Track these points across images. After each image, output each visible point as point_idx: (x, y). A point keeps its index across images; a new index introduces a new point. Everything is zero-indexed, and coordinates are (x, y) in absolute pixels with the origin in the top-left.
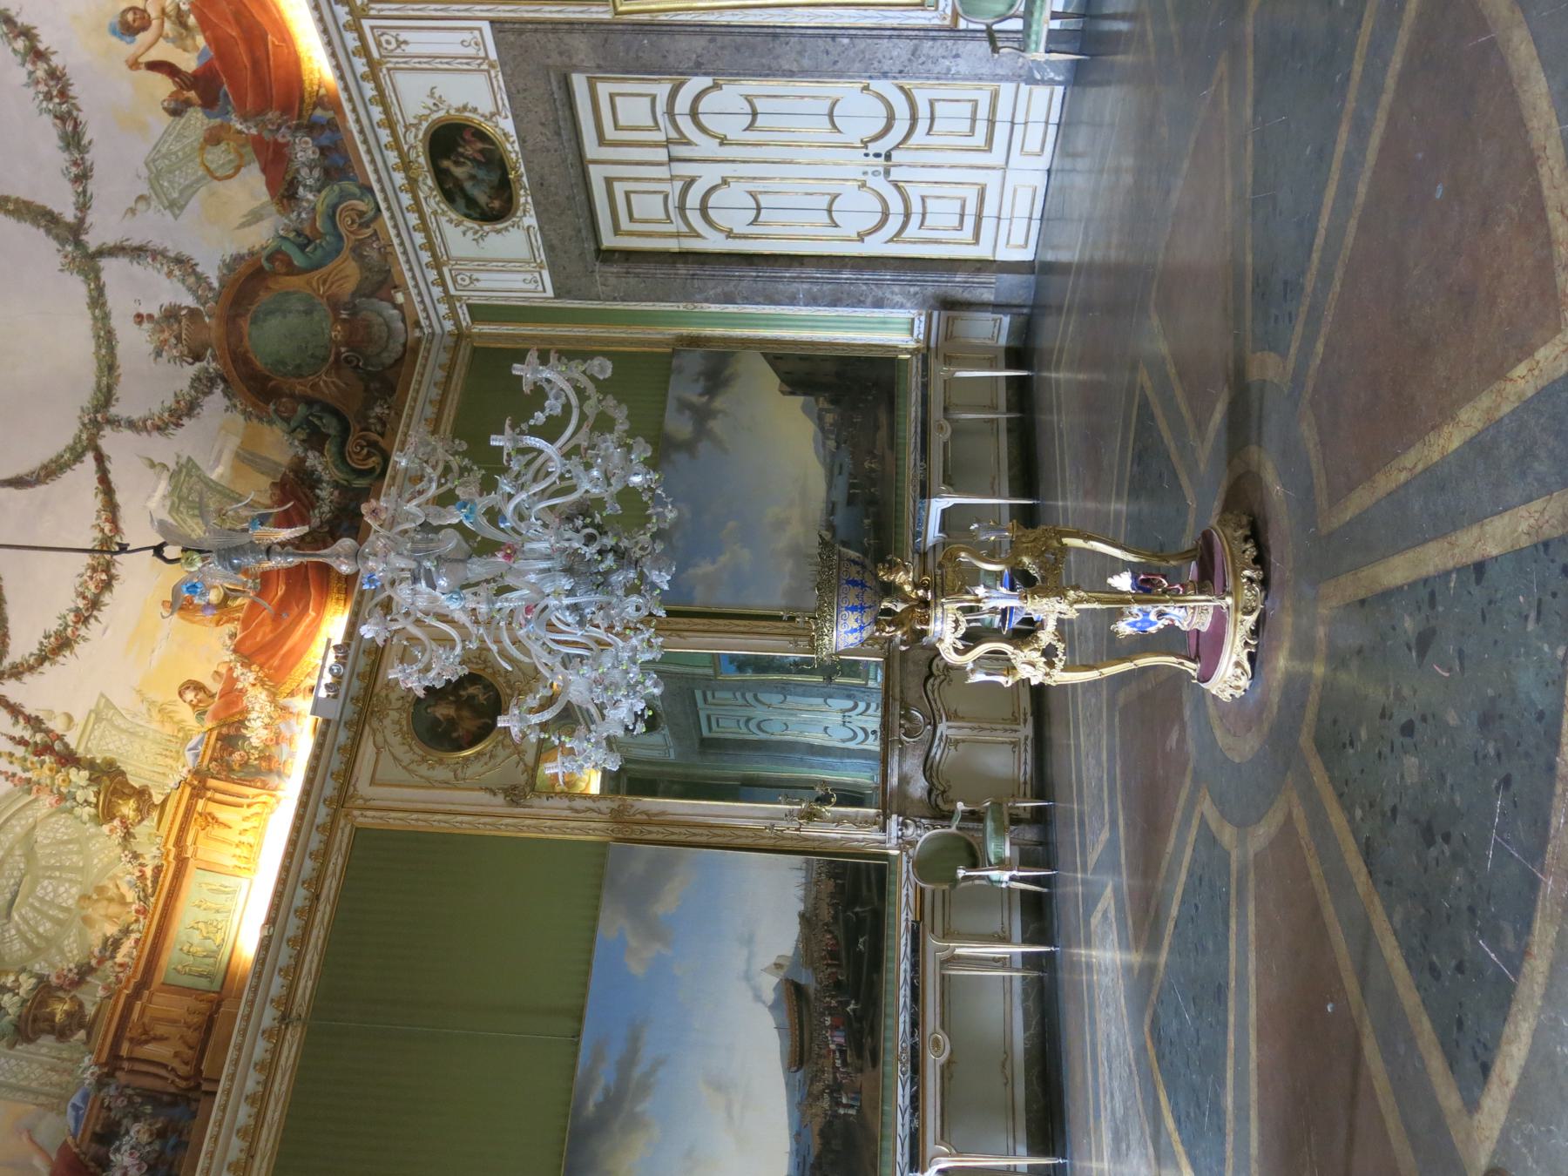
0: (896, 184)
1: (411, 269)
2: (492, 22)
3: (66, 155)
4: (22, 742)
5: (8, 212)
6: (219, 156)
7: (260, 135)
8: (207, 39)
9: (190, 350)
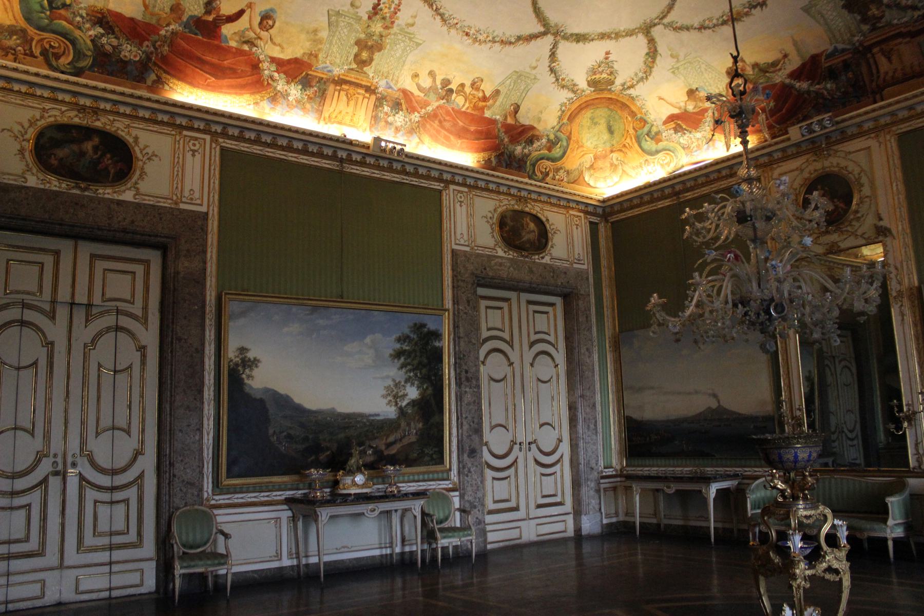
0: (45, 481)
1: (37, 75)
2: (207, 214)
7: (158, 34)
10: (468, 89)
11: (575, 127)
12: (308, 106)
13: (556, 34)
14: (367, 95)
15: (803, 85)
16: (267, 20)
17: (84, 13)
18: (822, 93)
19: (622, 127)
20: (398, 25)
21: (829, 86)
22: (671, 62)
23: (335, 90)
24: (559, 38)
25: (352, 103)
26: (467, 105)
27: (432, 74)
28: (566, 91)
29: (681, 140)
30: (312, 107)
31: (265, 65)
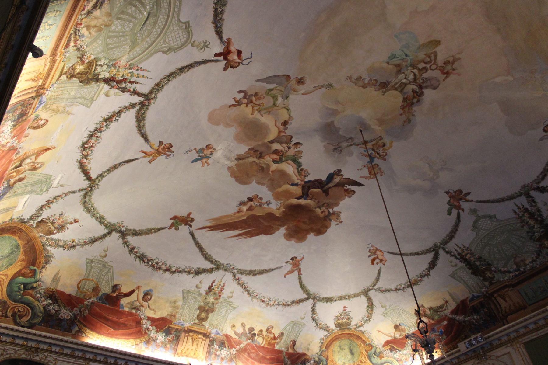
3: (141, 253)
4: (131, 82)
5: (153, 229)
6: (89, 286)
7: (83, 304)
8: (126, 311)
9: (45, 222)
10: (264, 333)
11: (330, 352)
12: (168, 346)
13: (314, 298)
14: (204, 339)
15: (461, 318)
16: (147, 295)
17: (42, 292)
18: (473, 322)
19: (358, 350)
20: (223, 297)
21: (475, 317)
22: (383, 310)
23: (185, 336)
24: (316, 300)
25: (195, 344)
26: (264, 342)
27: (243, 325)
28: (323, 331)
29: (395, 356)
30: (171, 347)
31: (144, 322)
